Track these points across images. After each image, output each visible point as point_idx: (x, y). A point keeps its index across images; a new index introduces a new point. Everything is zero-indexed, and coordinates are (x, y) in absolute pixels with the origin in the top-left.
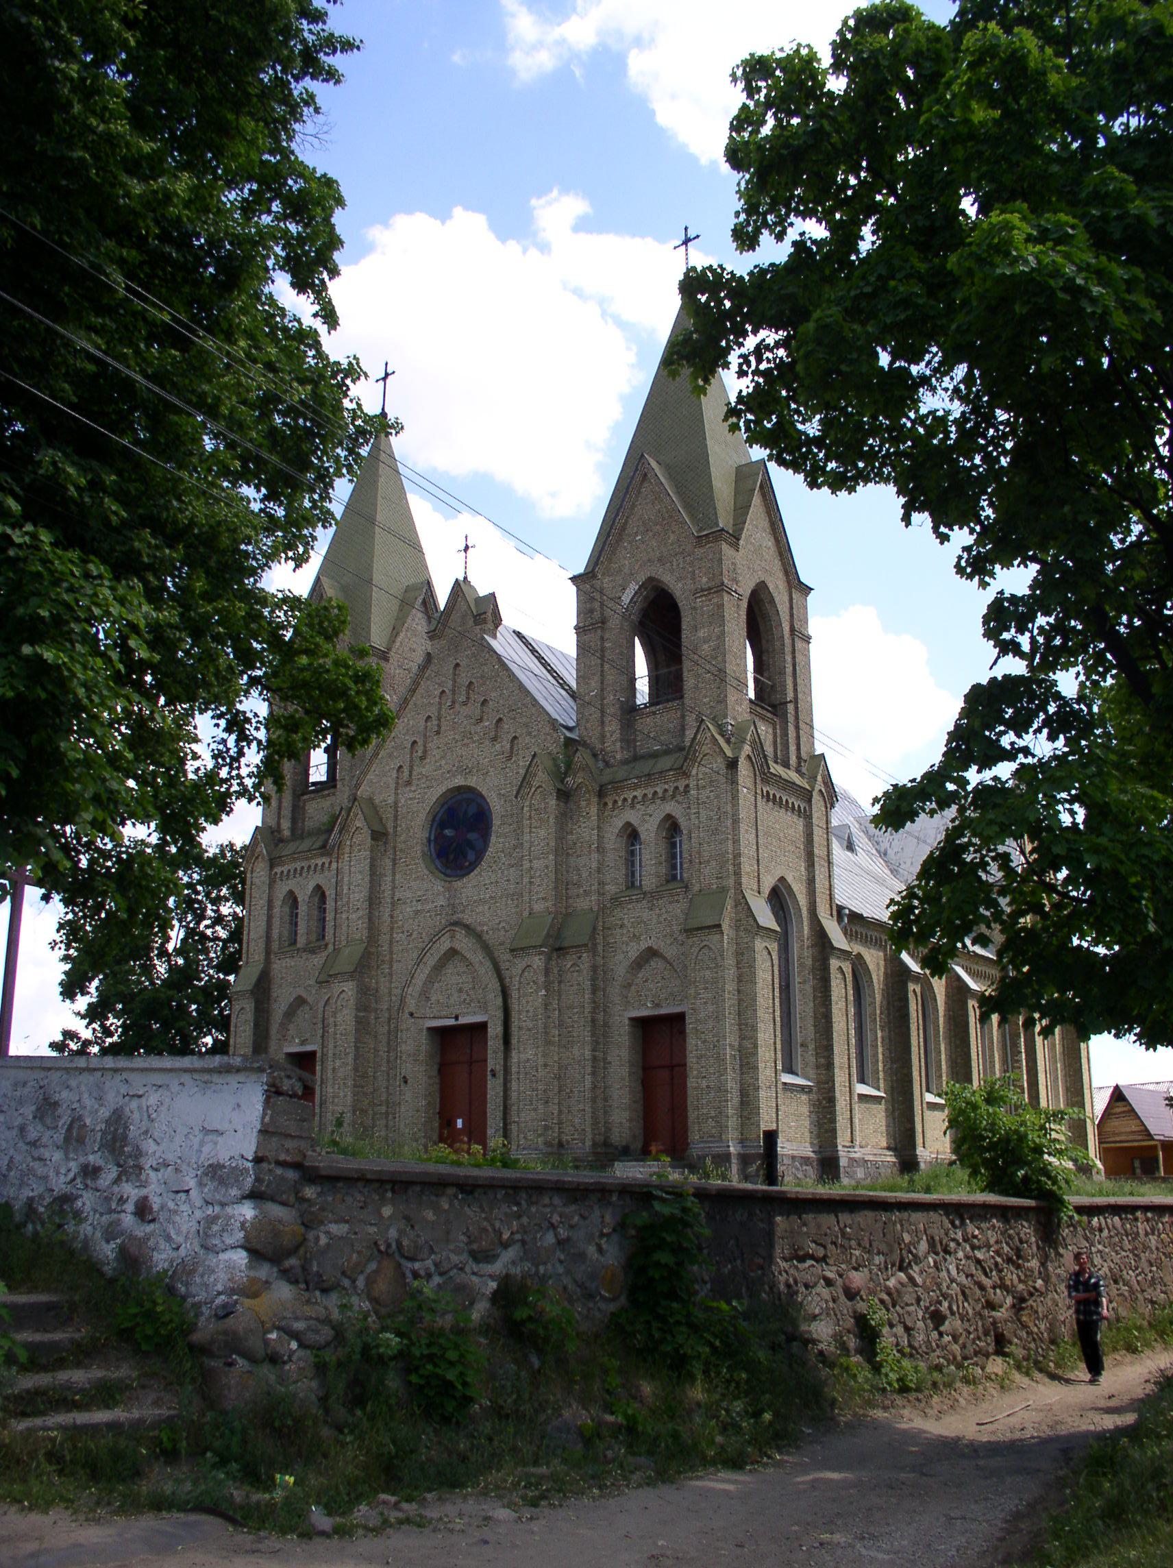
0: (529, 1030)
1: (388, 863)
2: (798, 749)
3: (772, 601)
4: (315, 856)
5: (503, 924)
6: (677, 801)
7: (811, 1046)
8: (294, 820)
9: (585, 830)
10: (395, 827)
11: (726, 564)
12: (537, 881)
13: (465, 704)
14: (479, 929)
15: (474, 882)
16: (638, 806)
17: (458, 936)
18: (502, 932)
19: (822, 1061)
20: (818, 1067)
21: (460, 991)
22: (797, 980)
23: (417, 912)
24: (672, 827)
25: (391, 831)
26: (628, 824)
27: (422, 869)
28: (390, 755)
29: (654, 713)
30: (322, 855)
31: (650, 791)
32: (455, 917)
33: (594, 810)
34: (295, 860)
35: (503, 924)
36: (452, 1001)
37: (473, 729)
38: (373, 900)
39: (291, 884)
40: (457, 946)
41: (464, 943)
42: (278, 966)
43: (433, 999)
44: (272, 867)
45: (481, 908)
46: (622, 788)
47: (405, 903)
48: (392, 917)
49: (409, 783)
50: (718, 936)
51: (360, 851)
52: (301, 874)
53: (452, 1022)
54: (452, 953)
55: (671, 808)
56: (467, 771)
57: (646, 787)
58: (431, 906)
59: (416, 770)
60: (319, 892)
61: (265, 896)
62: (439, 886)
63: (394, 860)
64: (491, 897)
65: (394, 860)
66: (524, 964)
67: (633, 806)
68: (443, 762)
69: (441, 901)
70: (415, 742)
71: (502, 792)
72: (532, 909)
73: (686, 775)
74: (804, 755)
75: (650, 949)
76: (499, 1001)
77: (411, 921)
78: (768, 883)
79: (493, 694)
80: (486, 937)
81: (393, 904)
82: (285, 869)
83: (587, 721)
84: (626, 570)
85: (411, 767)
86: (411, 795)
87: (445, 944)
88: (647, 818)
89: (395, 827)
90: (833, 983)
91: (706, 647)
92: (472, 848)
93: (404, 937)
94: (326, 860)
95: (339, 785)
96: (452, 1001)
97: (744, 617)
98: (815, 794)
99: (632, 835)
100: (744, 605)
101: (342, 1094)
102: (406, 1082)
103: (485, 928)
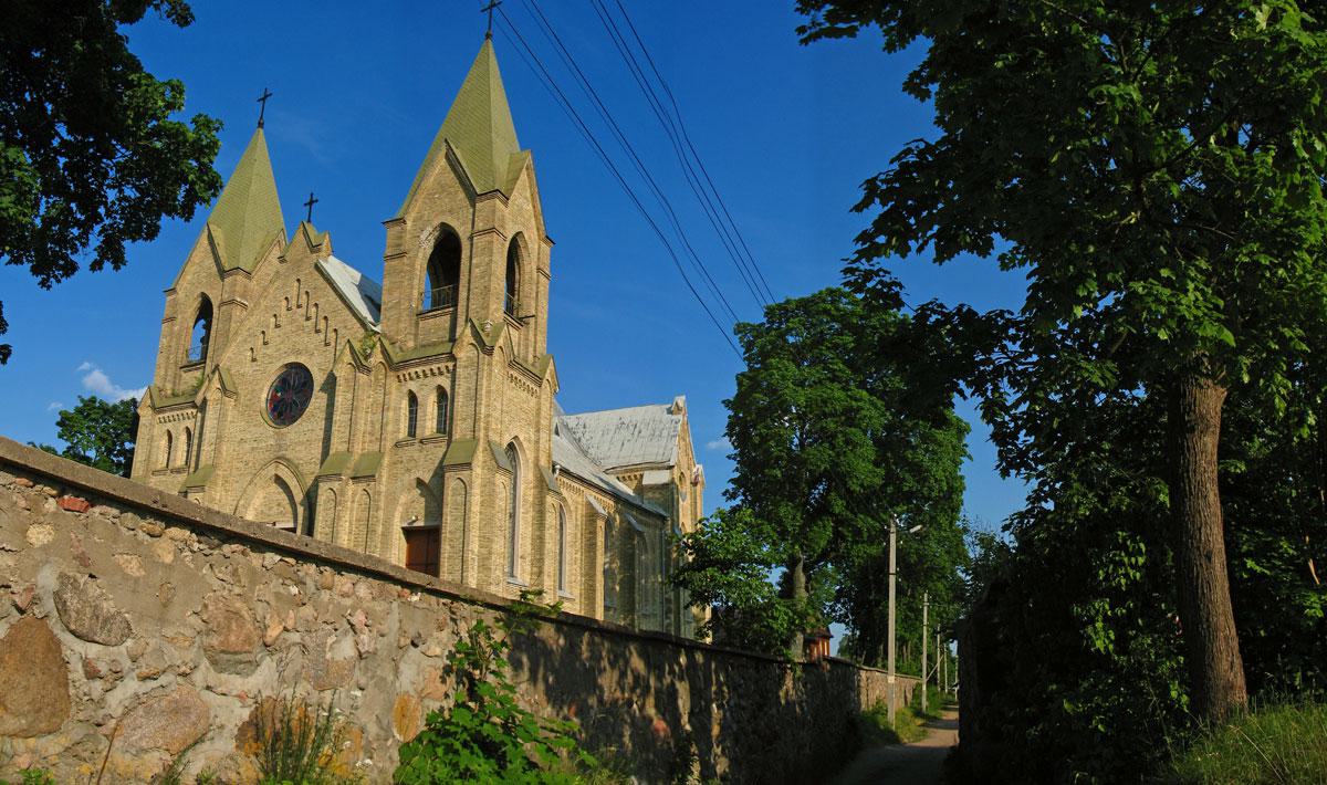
2: (535, 351)
3: (526, 247)
7: (529, 559)
11: (498, 214)
14: (296, 462)
19: (535, 569)
20: (532, 574)
21: (279, 505)
22: (522, 510)
23: (253, 449)
28: (245, 341)
31: (427, 368)
34: (172, 410)
39: (169, 426)
40: (280, 474)
50: (469, 472)
56: (299, 353)
74: (538, 355)
78: (507, 439)
84: (426, 218)
90: (548, 515)
91: (477, 270)
97: (506, 254)
98: (545, 381)
100: (507, 244)
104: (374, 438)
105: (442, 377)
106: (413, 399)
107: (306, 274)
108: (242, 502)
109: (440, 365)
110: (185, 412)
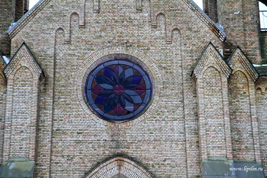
1: (49, 100)
12: (212, 134)
14: (144, 162)
17: (126, 165)
23: (78, 142)
25: (52, 75)
27: (85, 109)
32: (119, 151)
33: (252, 91)
35: (167, 162)
45: (145, 147)
47: (64, 133)
51: (24, 85)
58: (93, 138)
62: (101, 124)
64: (155, 140)
68: (103, 34)
70: (75, 14)
71: (163, 65)
81: (52, 131)
83: (233, 30)
86: (70, 52)
89: (55, 73)
93: (63, 160)
103: (151, 163)
104: (243, 147)
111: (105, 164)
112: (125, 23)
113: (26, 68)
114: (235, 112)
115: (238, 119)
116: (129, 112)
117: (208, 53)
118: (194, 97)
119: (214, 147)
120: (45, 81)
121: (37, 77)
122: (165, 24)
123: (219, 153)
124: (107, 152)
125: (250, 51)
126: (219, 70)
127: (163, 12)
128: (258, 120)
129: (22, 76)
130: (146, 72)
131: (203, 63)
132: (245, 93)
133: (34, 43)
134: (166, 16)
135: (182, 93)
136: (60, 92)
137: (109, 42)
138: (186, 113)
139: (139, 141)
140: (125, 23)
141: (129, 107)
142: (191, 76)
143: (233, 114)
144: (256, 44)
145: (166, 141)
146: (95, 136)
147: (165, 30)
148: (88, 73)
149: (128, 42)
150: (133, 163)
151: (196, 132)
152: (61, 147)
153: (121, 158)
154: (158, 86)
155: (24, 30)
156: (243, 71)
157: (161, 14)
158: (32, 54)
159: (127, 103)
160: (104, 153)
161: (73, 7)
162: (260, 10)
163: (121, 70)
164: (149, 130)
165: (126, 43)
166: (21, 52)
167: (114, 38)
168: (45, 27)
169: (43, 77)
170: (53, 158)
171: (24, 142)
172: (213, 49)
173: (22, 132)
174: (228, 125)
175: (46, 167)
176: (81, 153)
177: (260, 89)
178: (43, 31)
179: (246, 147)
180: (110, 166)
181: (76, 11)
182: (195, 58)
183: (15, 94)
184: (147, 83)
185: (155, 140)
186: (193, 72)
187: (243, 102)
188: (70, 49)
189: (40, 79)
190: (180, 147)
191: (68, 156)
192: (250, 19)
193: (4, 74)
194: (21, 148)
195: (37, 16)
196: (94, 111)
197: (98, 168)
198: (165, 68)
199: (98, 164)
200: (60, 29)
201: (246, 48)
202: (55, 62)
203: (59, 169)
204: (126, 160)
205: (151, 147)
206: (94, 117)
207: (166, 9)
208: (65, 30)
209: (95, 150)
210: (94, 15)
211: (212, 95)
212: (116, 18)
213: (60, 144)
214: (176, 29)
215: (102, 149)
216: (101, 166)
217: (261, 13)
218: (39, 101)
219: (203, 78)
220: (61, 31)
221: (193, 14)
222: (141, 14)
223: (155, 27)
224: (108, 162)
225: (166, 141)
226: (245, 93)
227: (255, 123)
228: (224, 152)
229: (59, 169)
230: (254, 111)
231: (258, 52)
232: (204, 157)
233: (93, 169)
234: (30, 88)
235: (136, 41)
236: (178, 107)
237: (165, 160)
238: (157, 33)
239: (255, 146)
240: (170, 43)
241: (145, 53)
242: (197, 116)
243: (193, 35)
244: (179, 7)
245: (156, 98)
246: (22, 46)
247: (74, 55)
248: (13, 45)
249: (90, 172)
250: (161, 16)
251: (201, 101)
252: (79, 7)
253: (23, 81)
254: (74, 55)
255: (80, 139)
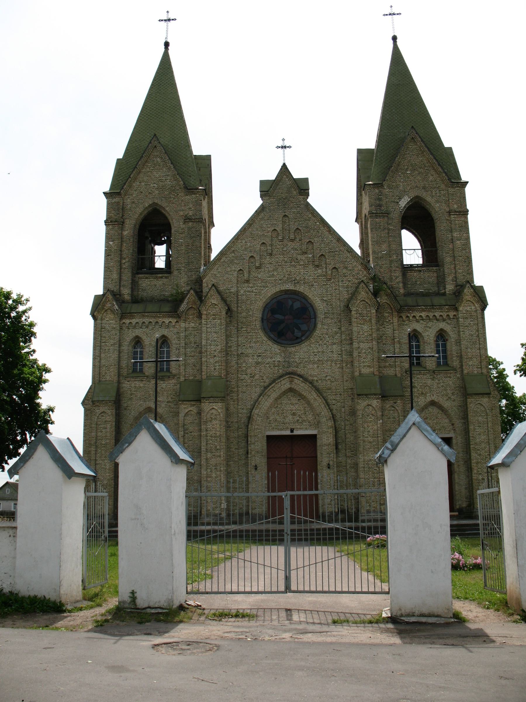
0: (370, 442)
1: (234, 331)
4: (164, 317)
5: (328, 378)
6: (447, 323)
8: (132, 289)
9: (388, 331)
10: (237, 307)
13: (292, 240)
15: (305, 349)
16: (421, 322)
17: (296, 381)
18: (329, 382)
21: (294, 414)
23: (258, 363)
24: (441, 335)
25: (235, 309)
26: (415, 330)
29: (420, 271)
30: (171, 317)
31: (431, 315)
32: (290, 370)
33: (395, 320)
35: (328, 378)
36: (287, 420)
37: (299, 257)
38: (227, 352)
41: (299, 385)
42: (126, 385)
43: (271, 418)
44: (121, 319)
46: (413, 310)
47: (247, 356)
48: (237, 363)
49: (247, 281)
51: (214, 319)
52: (147, 327)
53: (288, 433)
54: (291, 390)
55: (442, 325)
57: (429, 311)
58: (269, 360)
59: (254, 274)
60: (164, 341)
61: (117, 338)
62: (276, 348)
63: (237, 328)
64: (319, 360)
65: (237, 328)
66: (365, 403)
67: (417, 321)
69: (278, 358)
70: (252, 257)
71: (325, 299)
72: (360, 371)
73: (456, 309)
75: (433, 401)
76: (331, 423)
77: (253, 368)
79: (316, 239)
80: (315, 383)
82: (134, 321)
83: (381, 267)
85: (249, 272)
86: (249, 289)
87: (285, 384)
88: (428, 329)
89: (237, 307)
91: (458, 242)
92: (299, 329)
94: (174, 321)
95: (176, 273)
96: (287, 420)
99: (414, 336)
101: (214, 475)
102: (256, 469)
103: (315, 378)
104: (387, 364)
105: (444, 323)
106: (414, 336)
107: (294, 212)
108: (256, 411)
109: (441, 314)
110: (160, 320)
111: (279, 380)
112: (293, 263)
113: (216, 305)
114: (381, 337)
115: (384, 342)
116: (297, 338)
117: (360, 290)
118: (349, 325)
119: (365, 366)
120: (231, 314)
121: (224, 313)
122: (326, 264)
123: (368, 370)
124: (281, 371)
125: (395, 284)
126: (369, 303)
127: (324, 254)
128: (399, 342)
129: (213, 311)
130: (310, 304)
131: (356, 297)
132: (390, 321)
133: (220, 283)
134: (327, 257)
135: (340, 321)
136: (242, 323)
137: (280, 280)
138: (343, 338)
139: (306, 362)
140: (293, 263)
141: (297, 333)
142: (347, 307)
143: (379, 339)
144: (400, 279)
145: (327, 361)
146: (271, 358)
147: (326, 269)
148: (264, 306)
149: (295, 279)
150: (301, 379)
151: (351, 354)
152: (245, 367)
153: (292, 376)
154: (321, 316)
155: (212, 272)
156: (388, 302)
157: (322, 255)
158: (219, 292)
159: (296, 330)
160: (278, 371)
161: (250, 252)
162: (403, 248)
163: (290, 302)
164: (314, 352)
165: (294, 280)
166: (212, 292)
167: (284, 277)
168: (229, 269)
169: (229, 311)
170: (240, 376)
171: (217, 364)
172: (364, 286)
173: (215, 356)
174: (375, 347)
175: (233, 383)
176: (260, 372)
177: (401, 317)
178: (227, 273)
179: (390, 365)
180: (283, 382)
181: (253, 255)
182: (350, 292)
183: (208, 326)
184: (312, 313)
185: (319, 360)
186: (348, 305)
187: (388, 328)
188: (248, 287)
189: (227, 313)
190: (338, 365)
191: (251, 374)
192: (395, 257)
193: (199, 310)
194: (215, 369)
195: (222, 260)
196: (270, 338)
197: (274, 384)
198: (326, 301)
199: (274, 381)
200: (241, 270)
201: (392, 282)
202: (238, 298)
203: (245, 384)
204: (296, 377)
205: (316, 366)
206: (270, 343)
207: (327, 251)
208: (245, 271)
209: (271, 369)
210: (268, 257)
211: (364, 324)
212: (286, 259)
213: (244, 365)
214: (335, 268)
215: (276, 368)
216: (277, 382)
217: (404, 251)
218: (226, 330)
219: (356, 311)
220: (241, 272)
221: (349, 255)
222: (306, 255)
223: (317, 266)
224: (282, 379)
225: (327, 361)
226: (390, 321)
227: (397, 346)
228: (372, 370)
229: (245, 384)
230: (396, 335)
231: (401, 285)
232: (357, 374)
233: (270, 384)
234: (219, 321)
235: (302, 278)
236: (336, 333)
237: (326, 377)
238: (320, 271)
239: (397, 363)
240: (330, 280)
241: (310, 289)
242: (351, 340)
243: (349, 272)
244: (337, 249)
245: (319, 326)
246: (212, 286)
247: (252, 292)
248: (204, 285)
249: (268, 386)
250: (322, 257)
251: (355, 329)
252: (255, 251)
253: (213, 315)
254: (252, 292)
255: (260, 360)
